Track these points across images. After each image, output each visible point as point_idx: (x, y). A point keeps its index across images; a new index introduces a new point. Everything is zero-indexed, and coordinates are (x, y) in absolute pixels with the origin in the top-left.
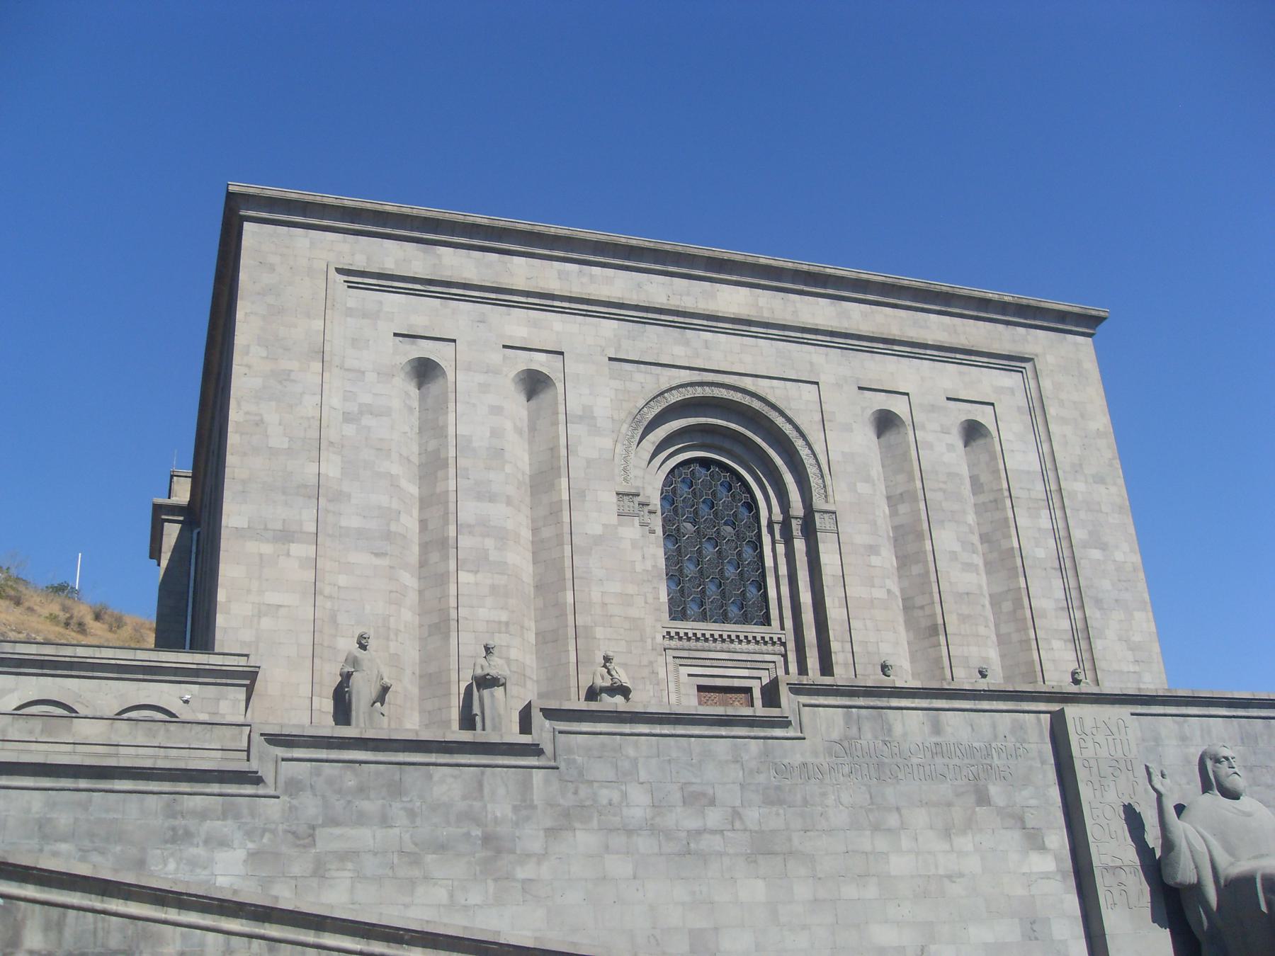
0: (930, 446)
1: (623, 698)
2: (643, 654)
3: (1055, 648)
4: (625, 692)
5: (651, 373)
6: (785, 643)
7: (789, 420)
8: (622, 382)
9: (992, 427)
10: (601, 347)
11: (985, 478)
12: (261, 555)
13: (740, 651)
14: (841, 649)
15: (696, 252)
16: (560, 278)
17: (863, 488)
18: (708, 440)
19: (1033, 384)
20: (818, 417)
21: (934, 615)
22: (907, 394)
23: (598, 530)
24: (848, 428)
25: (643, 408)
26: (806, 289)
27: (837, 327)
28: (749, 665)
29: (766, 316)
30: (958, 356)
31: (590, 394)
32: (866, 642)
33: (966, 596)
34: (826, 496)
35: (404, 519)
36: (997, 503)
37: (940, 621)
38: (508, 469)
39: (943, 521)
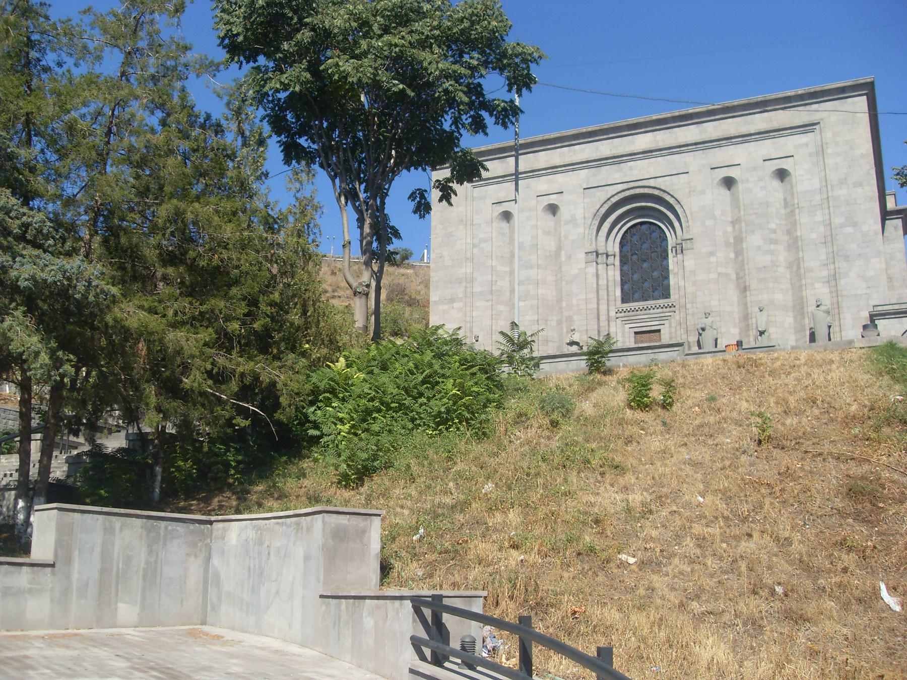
4: (577, 344)
7: (672, 196)
9: (790, 170)
11: (788, 200)
12: (444, 310)
15: (620, 124)
17: (709, 223)
19: (819, 137)
20: (687, 190)
23: (577, 272)
24: (703, 192)
26: (681, 124)
28: (658, 319)
29: (661, 145)
30: (771, 134)
35: (499, 283)
36: (793, 211)
38: (539, 252)
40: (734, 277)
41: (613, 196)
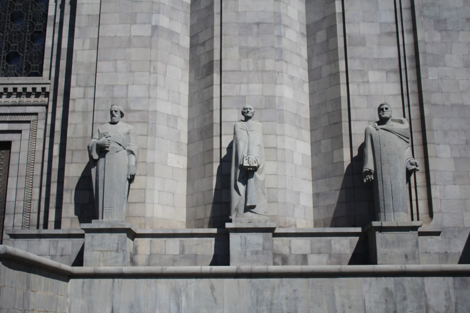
3: (370, 81)
14: (82, 96)
21: (211, 52)
28: (8, 118)
32: (113, 86)
33: (256, 27)
40: (186, 42)
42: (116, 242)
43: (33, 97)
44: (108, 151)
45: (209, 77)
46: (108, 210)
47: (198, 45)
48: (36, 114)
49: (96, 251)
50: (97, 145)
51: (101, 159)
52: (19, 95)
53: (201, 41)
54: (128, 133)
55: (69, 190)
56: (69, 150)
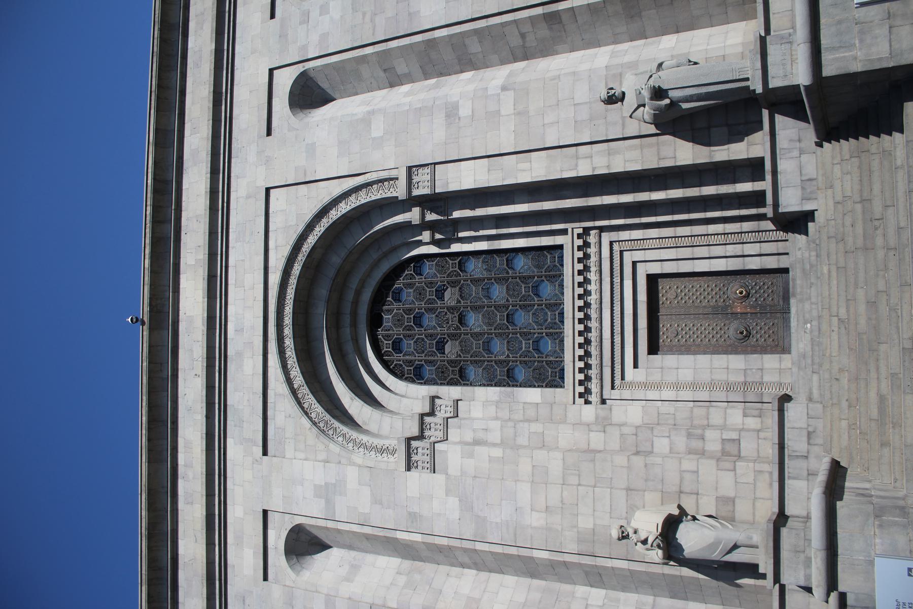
0: (324, 37)
1: (682, 526)
2: (612, 462)
5: (275, 403)
6: (584, 229)
7: (310, 227)
8: (287, 441)
10: (253, 464)
13: (598, 294)
14: (589, 160)
16: (192, 503)
17: (378, 129)
18: (347, 319)
22: (271, 71)
23: (453, 502)
24: (311, 149)
25: (310, 419)
27: (207, 168)
28: (617, 280)
31: (302, 485)
32: (575, 122)
34: (392, 179)
37: (539, 11)
39: (410, 14)
41: (289, 381)
42: (779, 46)
43: (589, 250)
44: (659, 86)
45: (565, 18)
46: (737, 73)
47: (524, 47)
48: (611, 243)
49: (792, 69)
50: (652, 99)
51: (670, 96)
52: (587, 268)
53: (520, 42)
54: (636, 74)
55: (710, 154)
56: (658, 164)
